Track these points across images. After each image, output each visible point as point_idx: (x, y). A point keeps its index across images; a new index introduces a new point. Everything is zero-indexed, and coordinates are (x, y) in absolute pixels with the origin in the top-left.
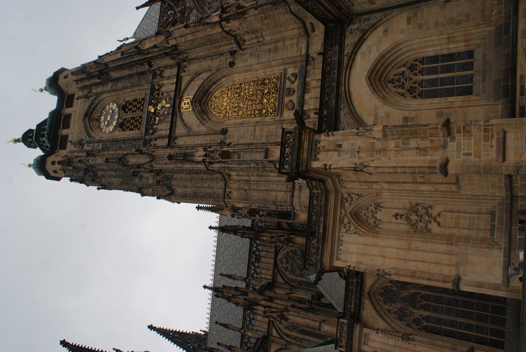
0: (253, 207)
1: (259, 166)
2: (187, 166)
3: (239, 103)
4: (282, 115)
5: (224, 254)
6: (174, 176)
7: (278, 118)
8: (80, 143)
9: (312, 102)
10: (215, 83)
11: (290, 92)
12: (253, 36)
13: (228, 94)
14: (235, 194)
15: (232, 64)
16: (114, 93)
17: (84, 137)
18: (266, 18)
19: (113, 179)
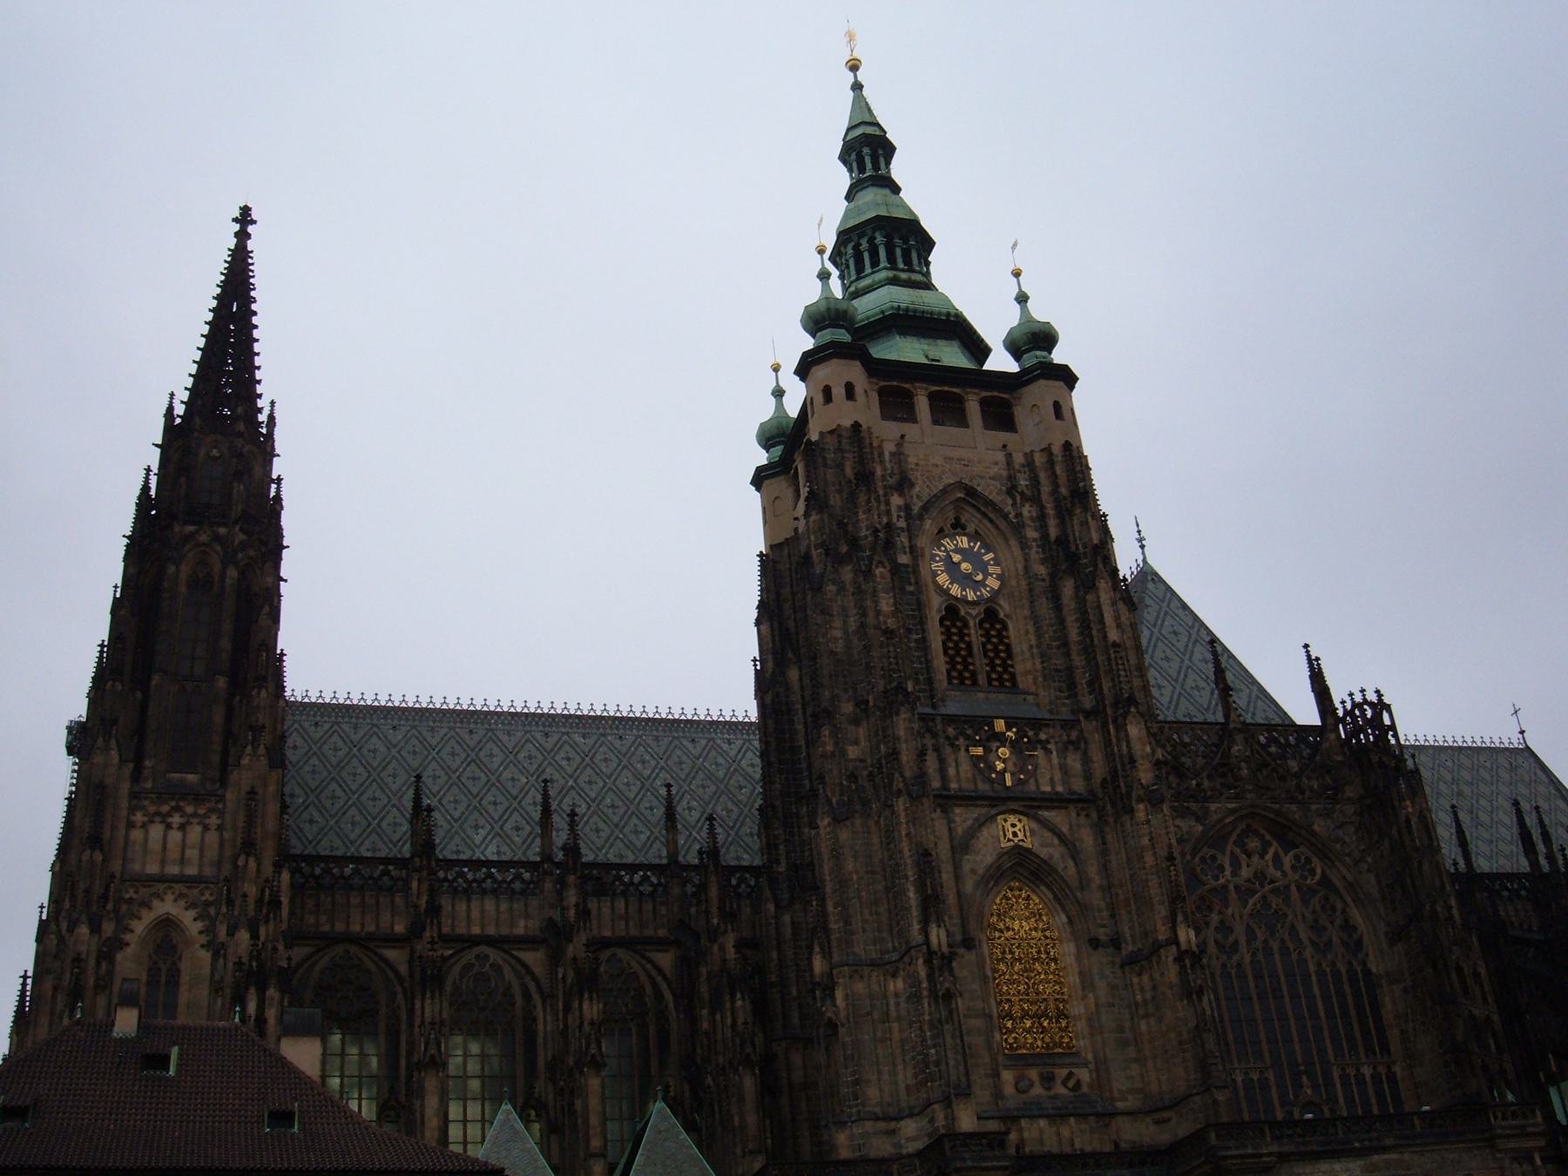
0: (842, 1031)
1: (933, 1068)
2: (911, 895)
3: (1020, 959)
4: (1006, 1067)
5: (567, 748)
6: (871, 823)
7: (1000, 1058)
8: (903, 484)
9: (1039, 1135)
10: (1056, 898)
11: (1048, 1080)
12: (1148, 995)
13: (1036, 929)
14: (860, 987)
15: (1095, 943)
16: (1024, 583)
17: (917, 489)
18: (1180, 1043)
19: (838, 623)
